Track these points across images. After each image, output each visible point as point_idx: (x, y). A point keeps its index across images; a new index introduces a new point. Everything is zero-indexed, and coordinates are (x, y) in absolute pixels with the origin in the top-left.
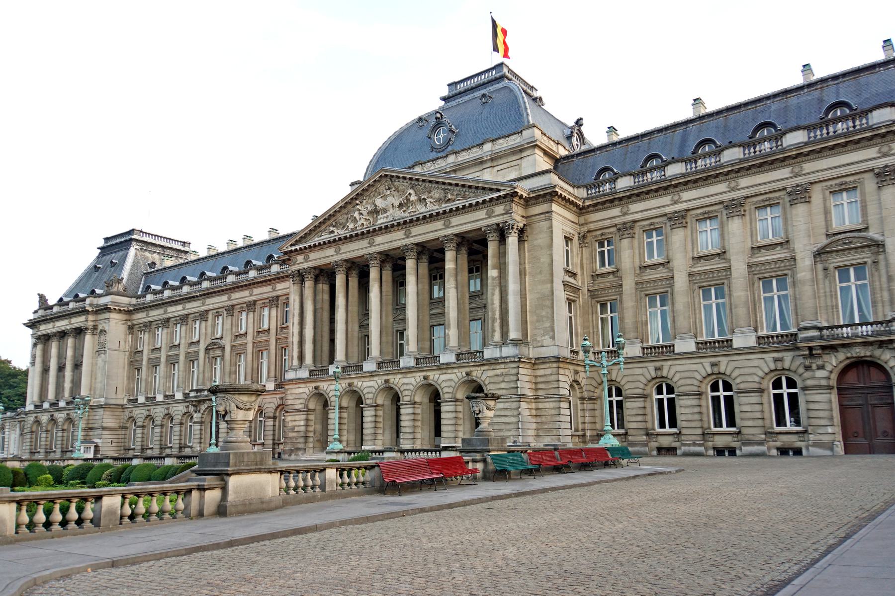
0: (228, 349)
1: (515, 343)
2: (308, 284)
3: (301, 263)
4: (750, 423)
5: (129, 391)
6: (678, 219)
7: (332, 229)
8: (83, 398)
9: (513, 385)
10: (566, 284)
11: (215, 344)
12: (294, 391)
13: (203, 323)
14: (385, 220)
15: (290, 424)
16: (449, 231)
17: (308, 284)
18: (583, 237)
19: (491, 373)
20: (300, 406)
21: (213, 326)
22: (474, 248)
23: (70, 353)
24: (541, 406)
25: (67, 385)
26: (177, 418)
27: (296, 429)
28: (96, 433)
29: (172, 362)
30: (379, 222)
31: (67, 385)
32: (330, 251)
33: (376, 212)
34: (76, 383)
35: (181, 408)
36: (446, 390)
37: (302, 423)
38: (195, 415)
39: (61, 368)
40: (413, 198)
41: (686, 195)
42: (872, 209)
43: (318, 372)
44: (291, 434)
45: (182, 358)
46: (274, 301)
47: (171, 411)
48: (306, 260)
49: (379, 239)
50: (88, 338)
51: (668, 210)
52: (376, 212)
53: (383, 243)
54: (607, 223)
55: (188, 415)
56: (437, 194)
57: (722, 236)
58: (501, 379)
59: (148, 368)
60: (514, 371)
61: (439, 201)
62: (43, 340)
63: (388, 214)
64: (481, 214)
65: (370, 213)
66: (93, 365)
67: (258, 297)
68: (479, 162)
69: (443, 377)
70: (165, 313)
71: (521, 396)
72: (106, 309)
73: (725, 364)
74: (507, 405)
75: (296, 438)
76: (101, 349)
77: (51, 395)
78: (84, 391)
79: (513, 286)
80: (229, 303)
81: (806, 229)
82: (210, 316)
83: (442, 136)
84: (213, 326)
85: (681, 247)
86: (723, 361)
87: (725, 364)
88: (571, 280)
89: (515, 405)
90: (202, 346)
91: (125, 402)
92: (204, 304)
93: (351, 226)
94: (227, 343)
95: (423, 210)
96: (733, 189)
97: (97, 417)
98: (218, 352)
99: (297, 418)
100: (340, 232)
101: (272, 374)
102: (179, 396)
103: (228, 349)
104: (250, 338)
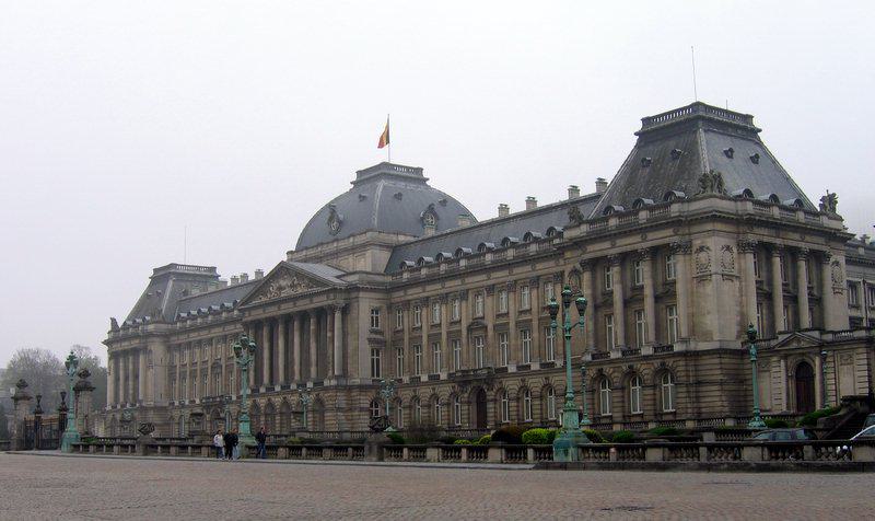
1: (337, 378)
5: (170, 395)
6: (426, 302)
8: (140, 402)
10: (370, 340)
16: (313, 306)
18: (390, 307)
23: (131, 367)
25: (131, 392)
29: (193, 375)
31: (131, 392)
32: (261, 311)
33: (280, 288)
34: (136, 389)
39: (127, 378)
41: (428, 288)
43: (255, 391)
50: (141, 358)
51: (421, 295)
52: (280, 288)
62: (114, 356)
66: (146, 377)
71: (339, 409)
72: (150, 335)
76: (149, 366)
77: (122, 399)
78: (140, 398)
88: (378, 337)
90: (210, 364)
94: (223, 362)
100: (264, 299)
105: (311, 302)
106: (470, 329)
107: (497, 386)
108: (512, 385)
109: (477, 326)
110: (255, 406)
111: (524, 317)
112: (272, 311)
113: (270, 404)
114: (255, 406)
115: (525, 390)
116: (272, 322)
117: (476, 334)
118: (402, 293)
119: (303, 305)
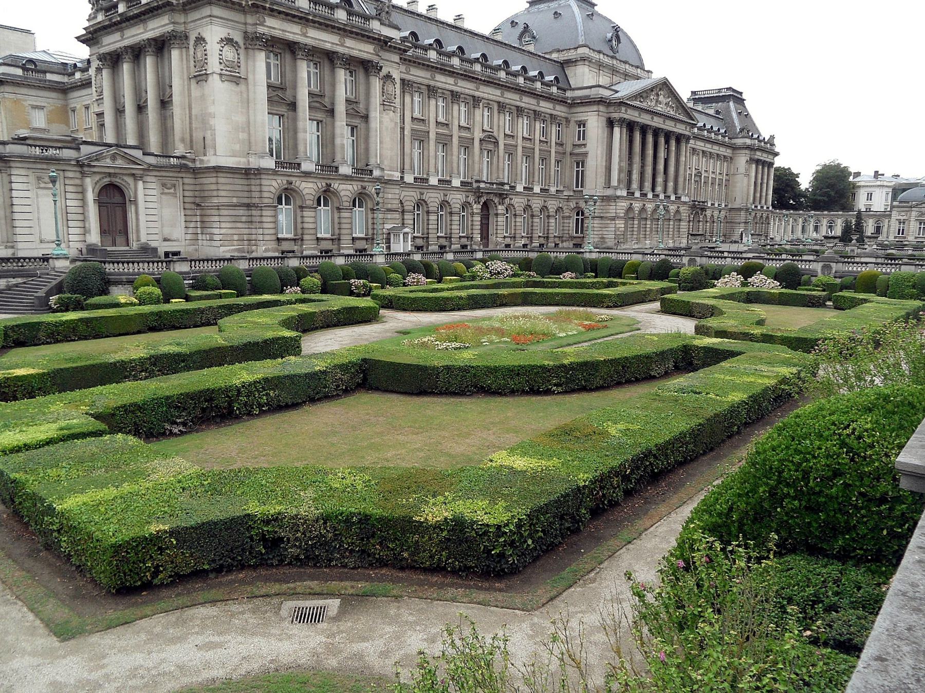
16: (675, 130)
26: (456, 207)
28: (389, 216)
32: (636, 114)
35: (459, 196)
38: (475, 206)
47: (448, 198)
55: (465, 206)
64: (683, 127)
70: (433, 79)
80: (501, 100)
92: (477, 89)
95: (672, 113)
97: (390, 196)
98: (491, 147)
102: (456, 183)
110: (630, 209)
112: (645, 119)
113: (643, 209)
114: (630, 209)
116: (644, 129)
119: (669, 126)
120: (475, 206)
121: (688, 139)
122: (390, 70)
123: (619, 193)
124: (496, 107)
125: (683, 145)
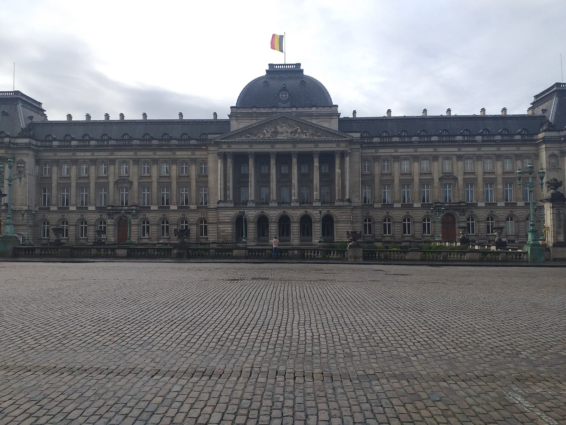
0: (136, 184)
1: (349, 200)
2: (229, 161)
3: (224, 148)
4: (417, 233)
6: (397, 159)
7: (248, 135)
9: (348, 217)
11: (124, 180)
12: (224, 213)
13: (112, 168)
14: (282, 138)
15: (222, 229)
16: (318, 149)
17: (229, 161)
19: (338, 212)
20: (228, 221)
21: (119, 169)
22: (327, 158)
24: (353, 225)
27: (226, 231)
28: (20, 228)
30: (279, 138)
32: (247, 146)
33: (276, 133)
36: (316, 217)
37: (230, 229)
40: (299, 131)
42: (455, 167)
44: (222, 234)
45: (92, 185)
46: (174, 161)
48: (229, 147)
49: (277, 146)
51: (394, 154)
52: (276, 133)
53: (279, 148)
54: (370, 154)
56: (311, 131)
57: (410, 167)
58: (343, 214)
59: (58, 190)
60: (350, 212)
61: (312, 135)
63: (284, 135)
64: (334, 145)
65: (273, 132)
67: (161, 157)
68: (311, 115)
69: (315, 212)
73: (411, 213)
74: (347, 225)
75: (227, 236)
79: (347, 178)
81: (436, 169)
82: (117, 163)
83: (284, 96)
84: (119, 169)
85: (397, 170)
86: (410, 211)
87: (411, 213)
89: (349, 225)
91: (37, 209)
92: (112, 155)
93: (262, 136)
95: (305, 137)
96: (416, 152)
99: (226, 226)
101: (174, 200)
103: (136, 184)
104: (154, 179)
105: (317, 147)
106: (440, 179)
107: (468, 214)
108: (482, 214)
109: (448, 179)
111: (488, 176)
115: (491, 217)
117: (445, 182)
118: (373, 151)
120: (109, 221)
121: (343, 155)
122: (23, 158)
123: (221, 205)
124: (131, 162)
125: (347, 159)
